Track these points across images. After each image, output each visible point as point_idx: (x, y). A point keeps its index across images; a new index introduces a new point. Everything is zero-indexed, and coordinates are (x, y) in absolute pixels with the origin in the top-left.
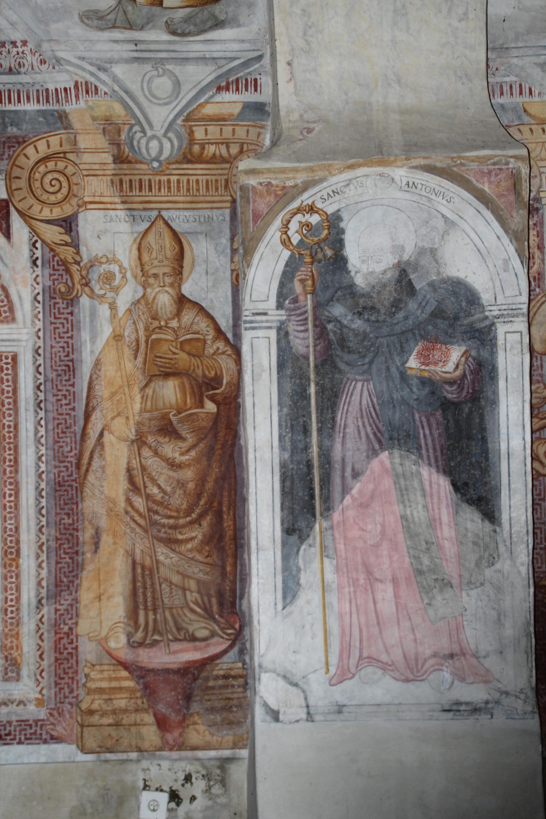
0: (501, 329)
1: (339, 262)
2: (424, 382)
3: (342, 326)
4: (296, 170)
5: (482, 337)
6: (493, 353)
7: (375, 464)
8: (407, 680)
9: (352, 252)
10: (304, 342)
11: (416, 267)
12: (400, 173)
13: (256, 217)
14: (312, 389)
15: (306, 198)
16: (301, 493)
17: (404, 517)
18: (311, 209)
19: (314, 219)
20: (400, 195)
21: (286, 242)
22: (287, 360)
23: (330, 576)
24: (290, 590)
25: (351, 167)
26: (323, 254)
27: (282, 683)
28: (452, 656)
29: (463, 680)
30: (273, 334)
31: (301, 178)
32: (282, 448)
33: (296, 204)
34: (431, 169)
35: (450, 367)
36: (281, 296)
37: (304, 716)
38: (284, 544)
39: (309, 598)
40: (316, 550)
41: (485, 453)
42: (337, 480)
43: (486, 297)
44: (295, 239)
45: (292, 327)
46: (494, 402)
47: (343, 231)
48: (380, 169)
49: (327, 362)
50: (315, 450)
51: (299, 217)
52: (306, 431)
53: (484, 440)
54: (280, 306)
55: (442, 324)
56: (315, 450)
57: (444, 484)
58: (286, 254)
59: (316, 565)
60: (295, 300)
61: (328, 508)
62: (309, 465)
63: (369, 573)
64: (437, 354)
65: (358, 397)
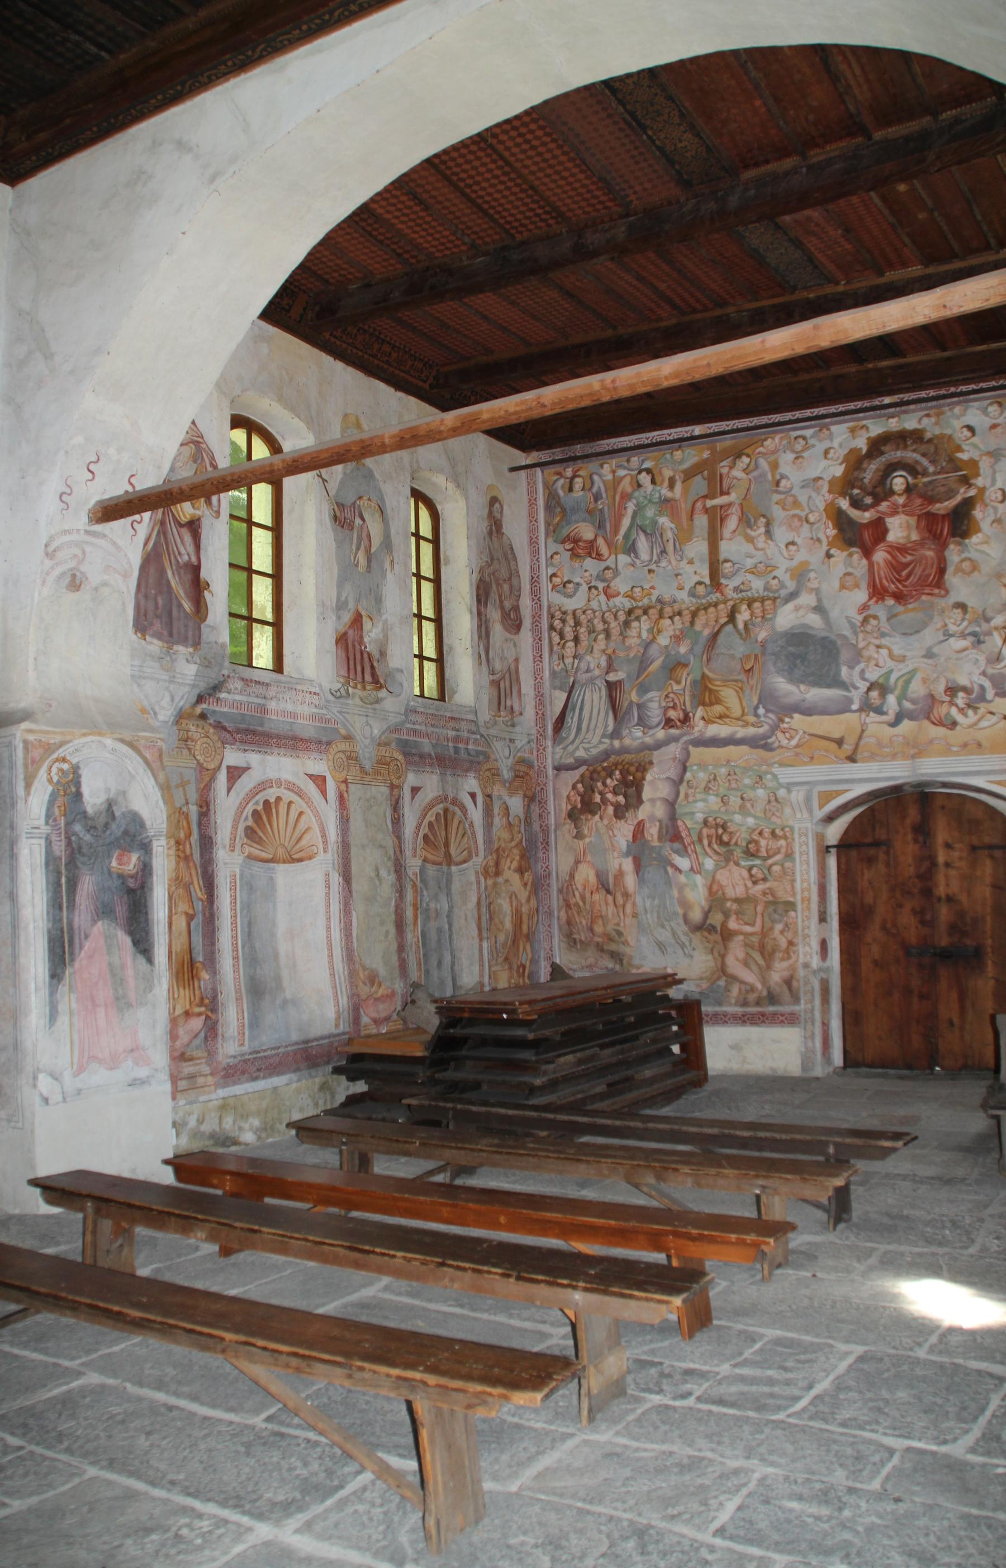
0: (155, 844)
1: (78, 795)
2: (121, 876)
3: (80, 839)
4: (54, 733)
5: (146, 848)
6: (151, 858)
7: (95, 929)
8: (111, 1069)
9: (85, 790)
10: (59, 848)
11: (116, 803)
12: (108, 742)
13: (33, 762)
14: (63, 880)
15: (60, 753)
16: (59, 951)
17: (110, 964)
18: (64, 760)
19: (66, 766)
20: (108, 755)
21: (50, 780)
22: (50, 860)
23: (74, 1005)
24: (53, 1015)
25: (84, 735)
26: (69, 791)
27: (49, 1079)
28: (132, 1050)
29: (137, 1064)
30: (43, 842)
31: (58, 739)
32: (48, 920)
33: (55, 756)
34: (122, 741)
35: (131, 866)
36: (48, 816)
37: (61, 1099)
38: (50, 985)
39: (63, 1020)
40: (67, 988)
41: (147, 920)
42: (77, 941)
43: (148, 824)
44: (55, 779)
45: (54, 838)
46: (151, 889)
47: (80, 776)
48: (98, 738)
49: (72, 862)
50: (65, 920)
51: (57, 764)
52: (61, 908)
53: (146, 913)
54: (47, 823)
55: (128, 839)
56: (65, 920)
57: (127, 941)
58: (50, 788)
59: (67, 999)
60: (55, 820)
61: (72, 960)
62: (62, 931)
63: (93, 1001)
64: (125, 859)
65: (88, 884)
